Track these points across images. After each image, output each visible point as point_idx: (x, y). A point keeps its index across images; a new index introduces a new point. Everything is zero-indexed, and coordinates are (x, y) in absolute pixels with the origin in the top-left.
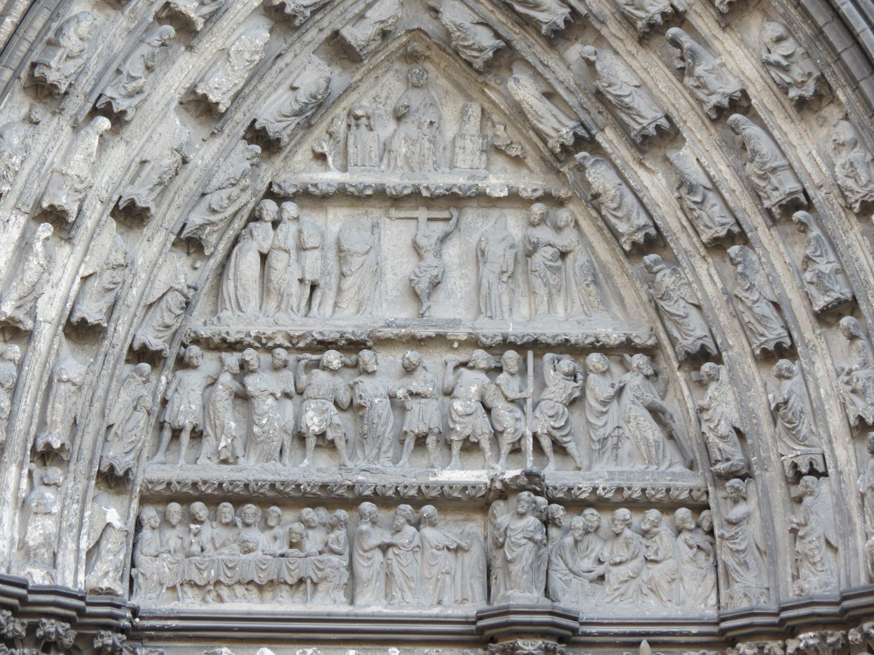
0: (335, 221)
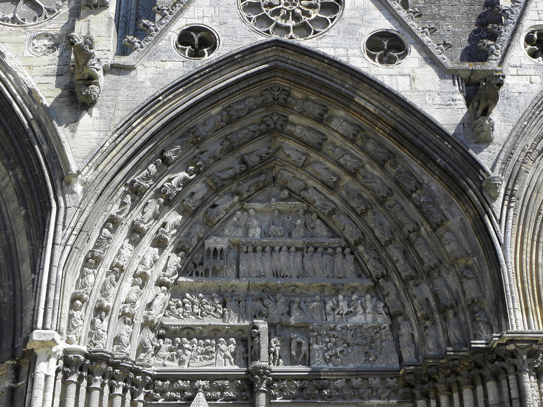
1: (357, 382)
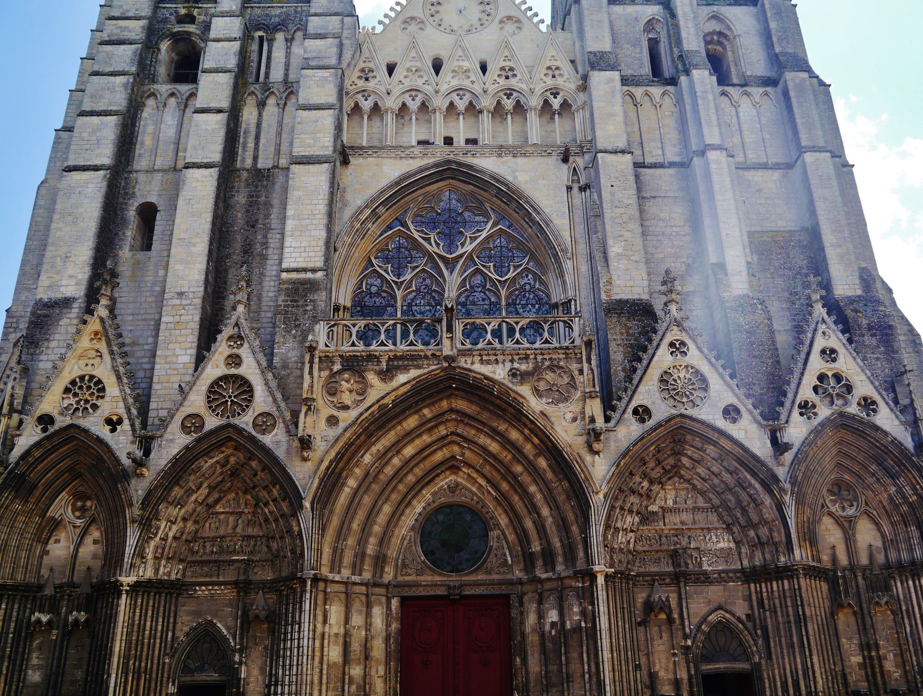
0: (222, 517)
1: (723, 575)
